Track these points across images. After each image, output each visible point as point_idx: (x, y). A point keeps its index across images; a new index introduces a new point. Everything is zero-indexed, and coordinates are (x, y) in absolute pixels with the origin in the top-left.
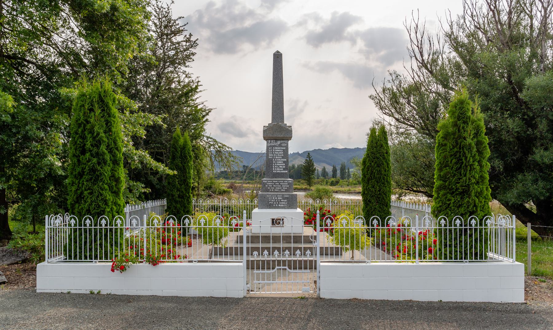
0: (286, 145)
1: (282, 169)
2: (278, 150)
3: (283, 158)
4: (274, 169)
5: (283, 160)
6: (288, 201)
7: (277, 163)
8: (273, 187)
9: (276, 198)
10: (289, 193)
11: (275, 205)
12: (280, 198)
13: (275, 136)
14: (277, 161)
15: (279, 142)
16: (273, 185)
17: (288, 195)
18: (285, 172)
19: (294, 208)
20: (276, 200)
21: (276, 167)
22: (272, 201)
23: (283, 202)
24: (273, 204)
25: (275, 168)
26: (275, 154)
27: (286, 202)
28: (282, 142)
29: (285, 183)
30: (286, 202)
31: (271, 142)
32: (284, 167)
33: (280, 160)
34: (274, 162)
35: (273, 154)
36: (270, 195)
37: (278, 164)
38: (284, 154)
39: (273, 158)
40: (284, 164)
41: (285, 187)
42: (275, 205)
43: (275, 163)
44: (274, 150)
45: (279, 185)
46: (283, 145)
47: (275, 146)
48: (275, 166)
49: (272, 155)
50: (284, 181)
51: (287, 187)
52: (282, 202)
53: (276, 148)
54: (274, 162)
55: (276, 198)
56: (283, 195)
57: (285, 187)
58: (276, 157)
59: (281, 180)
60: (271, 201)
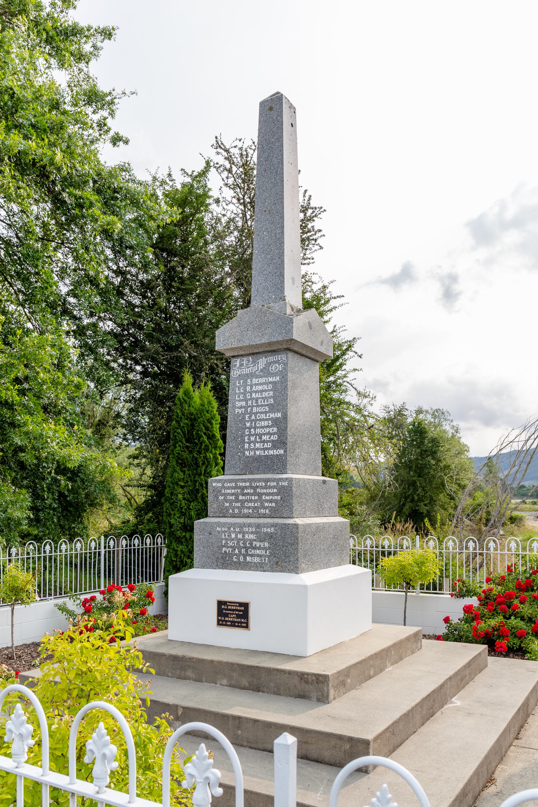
0: (280, 367)
1: (270, 445)
2: (260, 388)
3: (272, 408)
4: (247, 446)
5: (272, 415)
6: (274, 547)
7: (255, 428)
8: (237, 500)
9: (240, 536)
10: (276, 521)
11: (238, 556)
12: (252, 537)
13: (247, 343)
14: (256, 420)
15: (262, 362)
16: (236, 495)
17: (272, 525)
18: (276, 452)
19: (290, 571)
20: (239, 540)
21: (253, 439)
22: (231, 544)
23: (259, 548)
24: (231, 555)
25: (249, 443)
26: (252, 399)
27: (265, 549)
28: (271, 359)
29: (271, 487)
30: (265, 549)
31: (241, 365)
32: (275, 438)
33: (263, 416)
34: (248, 425)
35: (246, 401)
36: (223, 525)
37: (258, 431)
38: (274, 397)
39: (246, 411)
40: (275, 430)
41: (271, 501)
42: (238, 556)
43: (250, 428)
44: (248, 388)
45: (255, 494)
46: (273, 368)
47: (252, 375)
48: (249, 435)
49: (244, 403)
50: (266, 481)
51: (276, 501)
52: (255, 548)
53: (255, 381)
54: (248, 425)
55: (240, 536)
56: (258, 526)
57: (271, 501)
58: (255, 410)
59: (260, 480)
60: (226, 546)
